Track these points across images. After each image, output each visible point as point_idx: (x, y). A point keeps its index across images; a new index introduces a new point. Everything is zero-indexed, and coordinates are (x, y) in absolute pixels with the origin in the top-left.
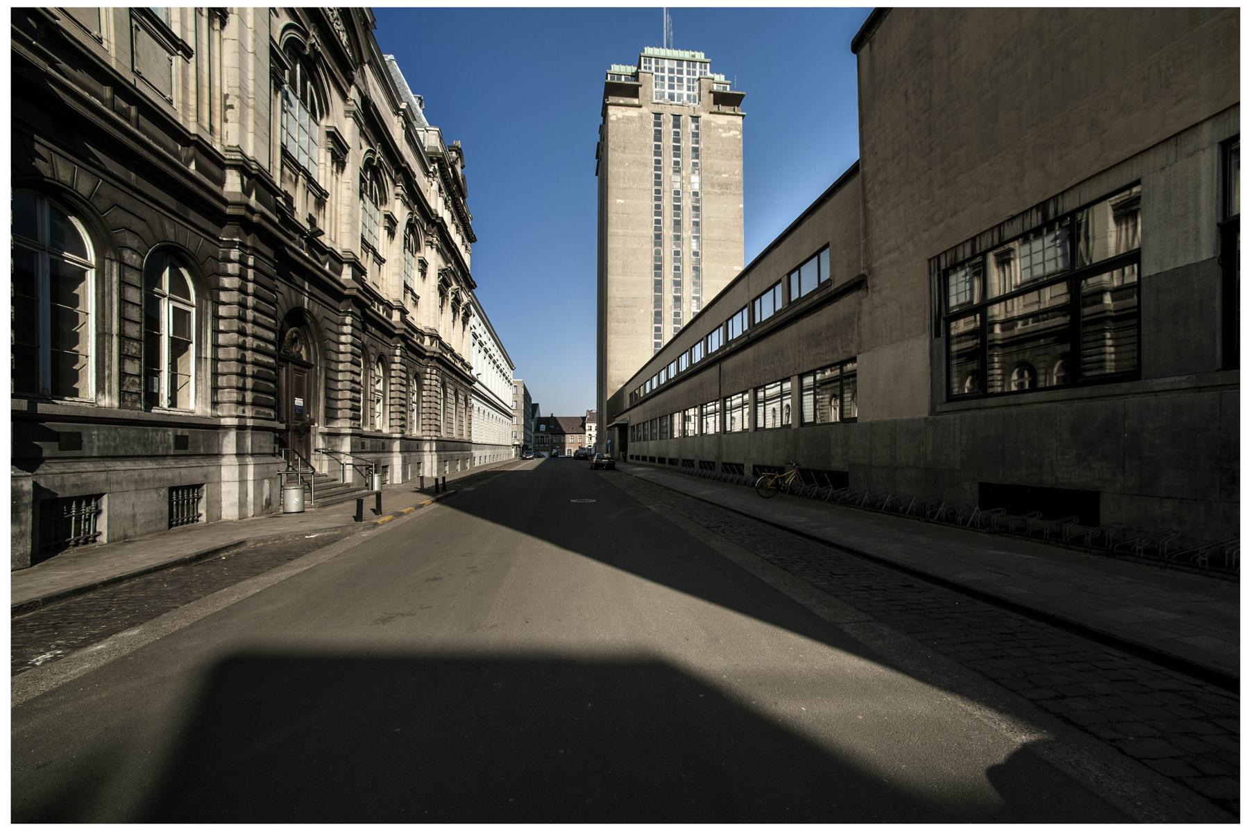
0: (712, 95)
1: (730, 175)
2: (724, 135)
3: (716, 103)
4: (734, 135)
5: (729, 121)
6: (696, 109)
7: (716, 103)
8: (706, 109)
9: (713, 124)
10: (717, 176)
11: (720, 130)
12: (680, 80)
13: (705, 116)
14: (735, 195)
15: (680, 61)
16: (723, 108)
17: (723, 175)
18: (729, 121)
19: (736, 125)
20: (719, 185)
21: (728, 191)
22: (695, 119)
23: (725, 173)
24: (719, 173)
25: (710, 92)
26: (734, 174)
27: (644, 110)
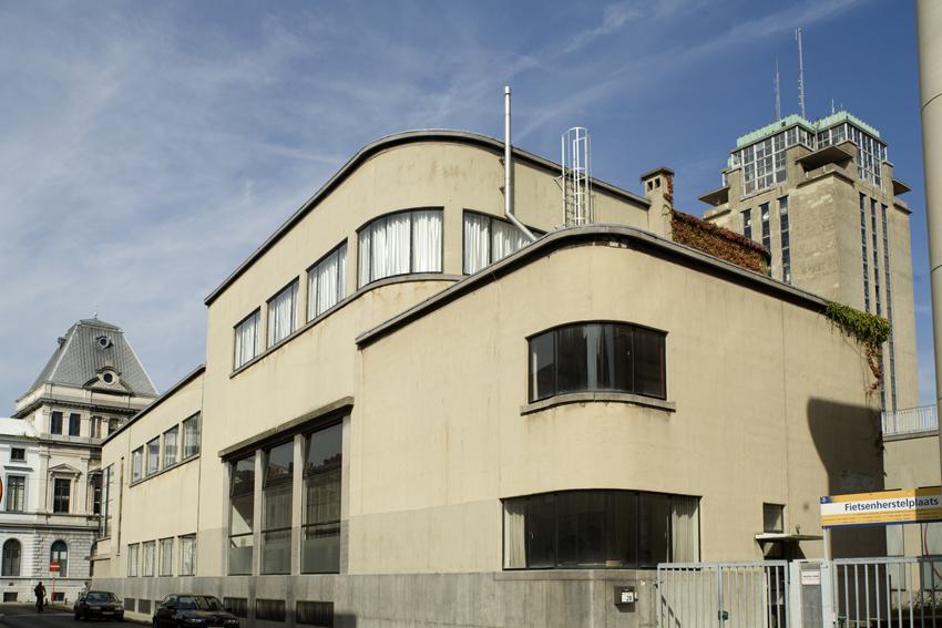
0: (799, 166)
2: (813, 206)
3: (806, 169)
4: (826, 201)
9: (801, 198)
13: (792, 192)
14: (828, 273)
16: (815, 173)
17: (815, 255)
19: (829, 186)
21: (821, 273)
22: (783, 200)
23: (818, 250)
24: (810, 254)
25: (797, 163)
26: (827, 249)
27: (734, 212)
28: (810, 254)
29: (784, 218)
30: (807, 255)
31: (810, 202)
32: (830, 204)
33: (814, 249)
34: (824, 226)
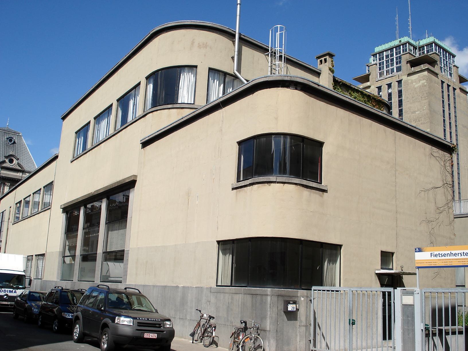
1: (421, 112)
2: (416, 86)
3: (412, 66)
4: (423, 84)
5: (419, 76)
6: (400, 76)
7: (412, 66)
8: (405, 74)
9: (410, 81)
10: (413, 115)
11: (414, 84)
12: (392, 60)
13: (404, 78)
14: (424, 123)
15: (391, 49)
17: (416, 113)
18: (419, 76)
19: (424, 76)
20: (414, 120)
22: (400, 82)
23: (418, 110)
24: (414, 112)
26: (424, 110)
28: (414, 112)
29: (400, 92)
30: (412, 113)
31: (414, 84)
32: (425, 86)
33: (416, 109)
34: (422, 97)
